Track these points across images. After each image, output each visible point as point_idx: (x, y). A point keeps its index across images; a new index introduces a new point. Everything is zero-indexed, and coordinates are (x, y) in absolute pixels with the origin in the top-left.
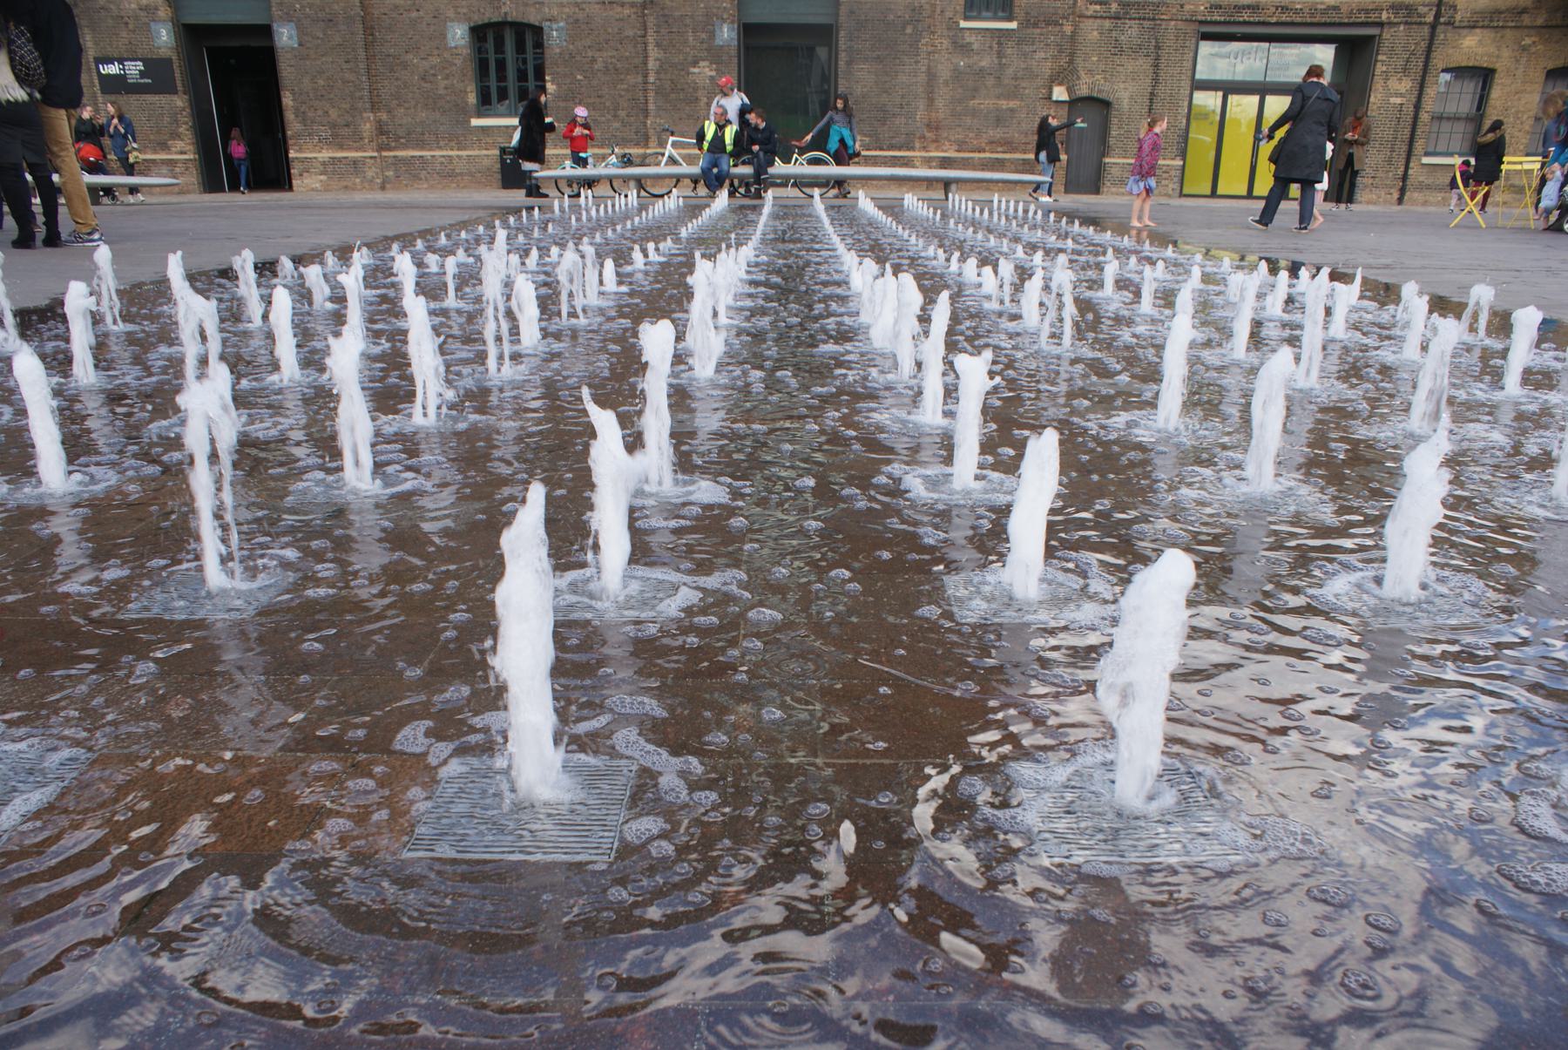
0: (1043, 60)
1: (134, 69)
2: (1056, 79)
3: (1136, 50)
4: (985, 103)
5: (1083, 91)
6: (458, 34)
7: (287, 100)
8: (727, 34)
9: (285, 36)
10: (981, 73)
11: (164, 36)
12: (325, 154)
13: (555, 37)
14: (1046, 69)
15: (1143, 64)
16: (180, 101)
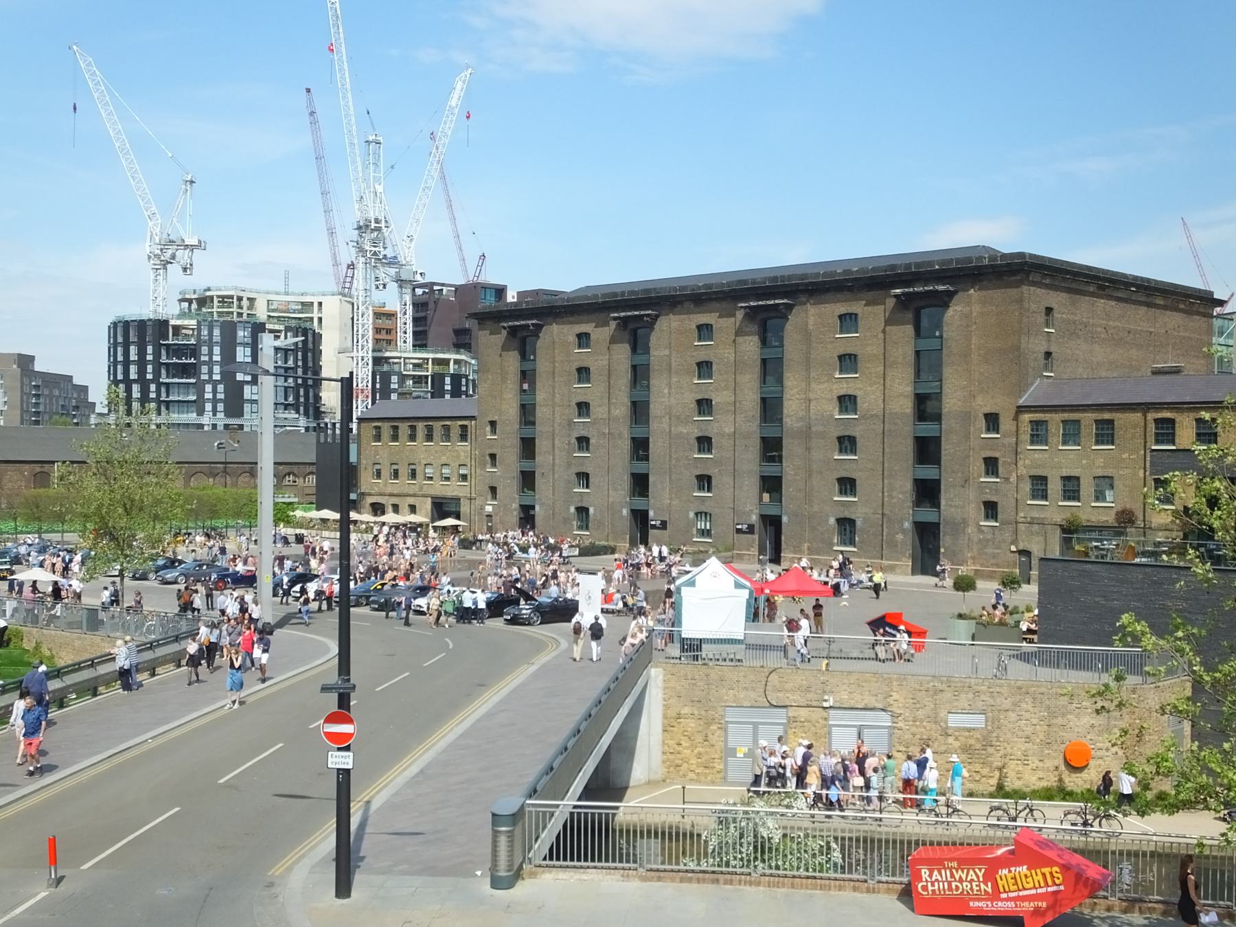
0: (1008, 536)
1: (745, 526)
2: (1012, 543)
3: (1038, 533)
4: (989, 550)
5: (1021, 548)
6: (832, 521)
7: (783, 538)
8: (907, 525)
9: (785, 519)
10: (988, 540)
11: (754, 518)
12: (791, 555)
13: (859, 523)
14: (1010, 539)
15: (1041, 539)
16: (756, 537)
